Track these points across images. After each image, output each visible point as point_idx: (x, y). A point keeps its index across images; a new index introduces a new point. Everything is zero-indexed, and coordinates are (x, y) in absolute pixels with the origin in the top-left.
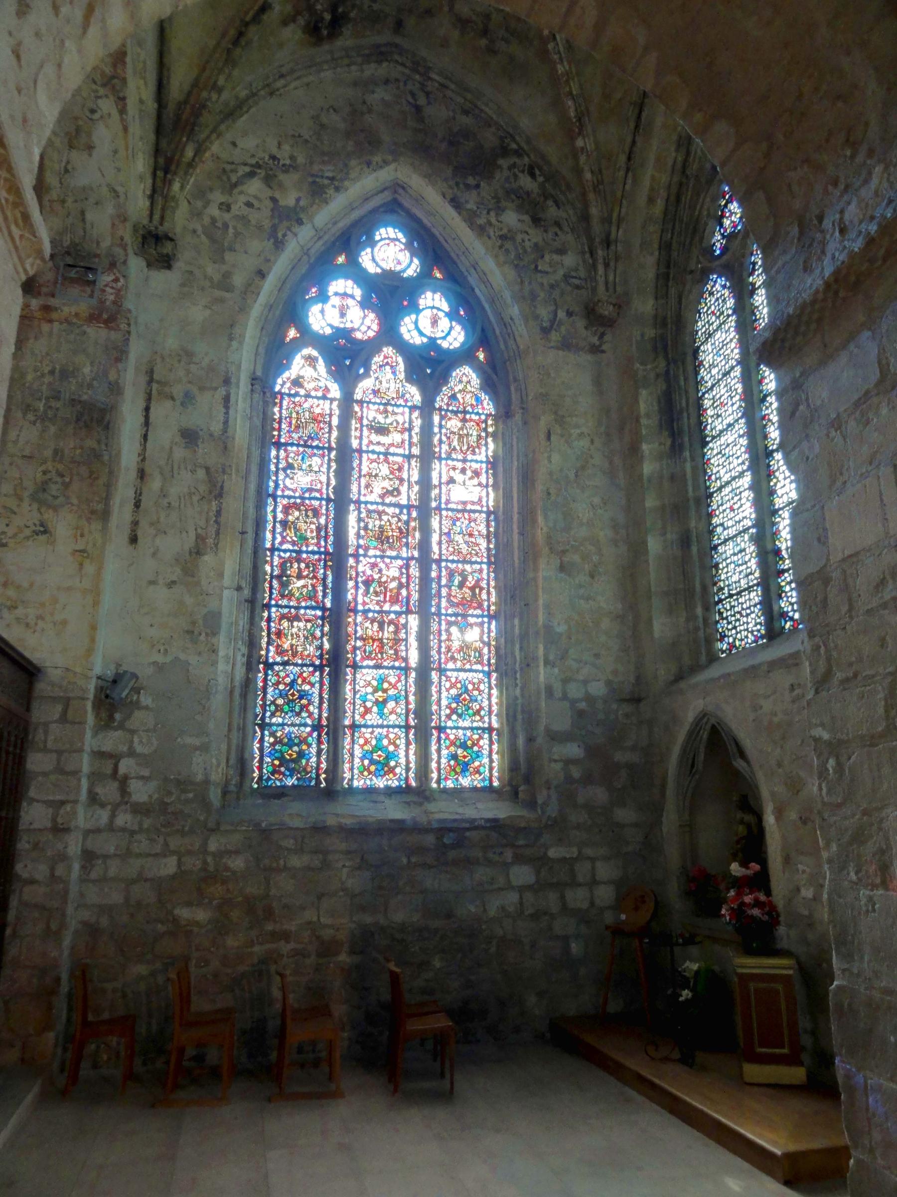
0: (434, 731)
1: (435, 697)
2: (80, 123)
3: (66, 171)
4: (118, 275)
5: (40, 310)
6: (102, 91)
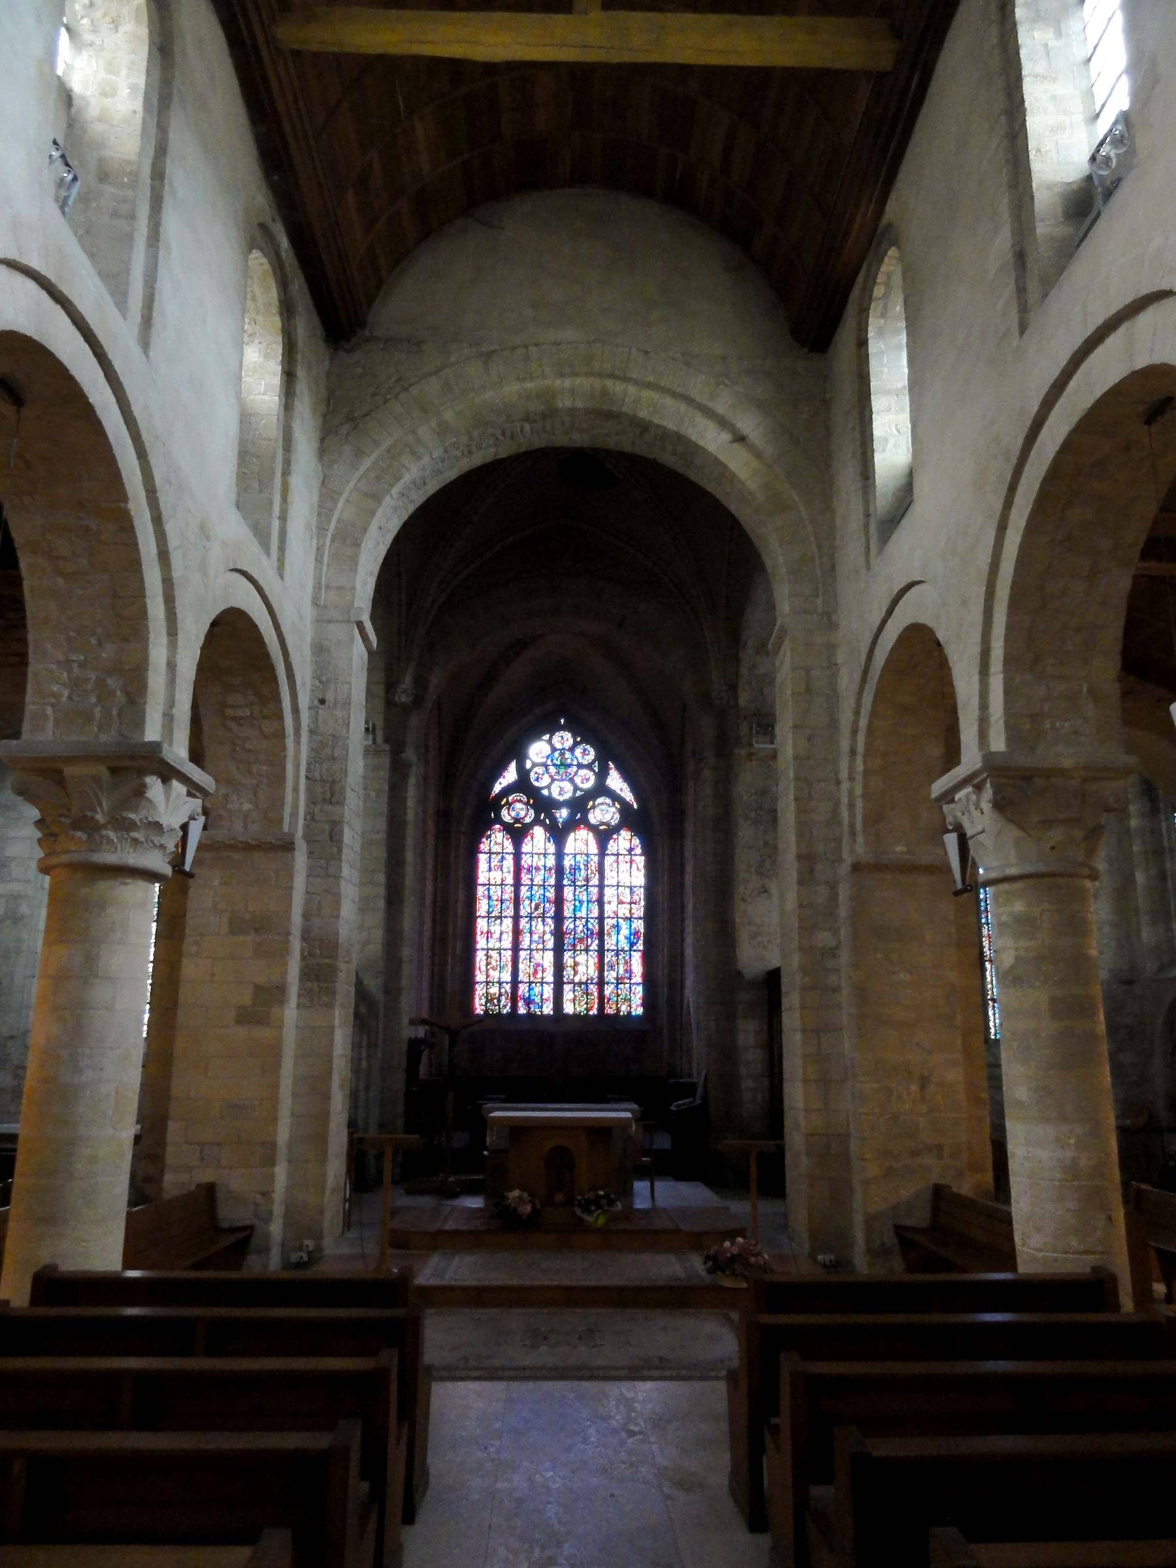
0: (990, 1002)
1: (989, 979)
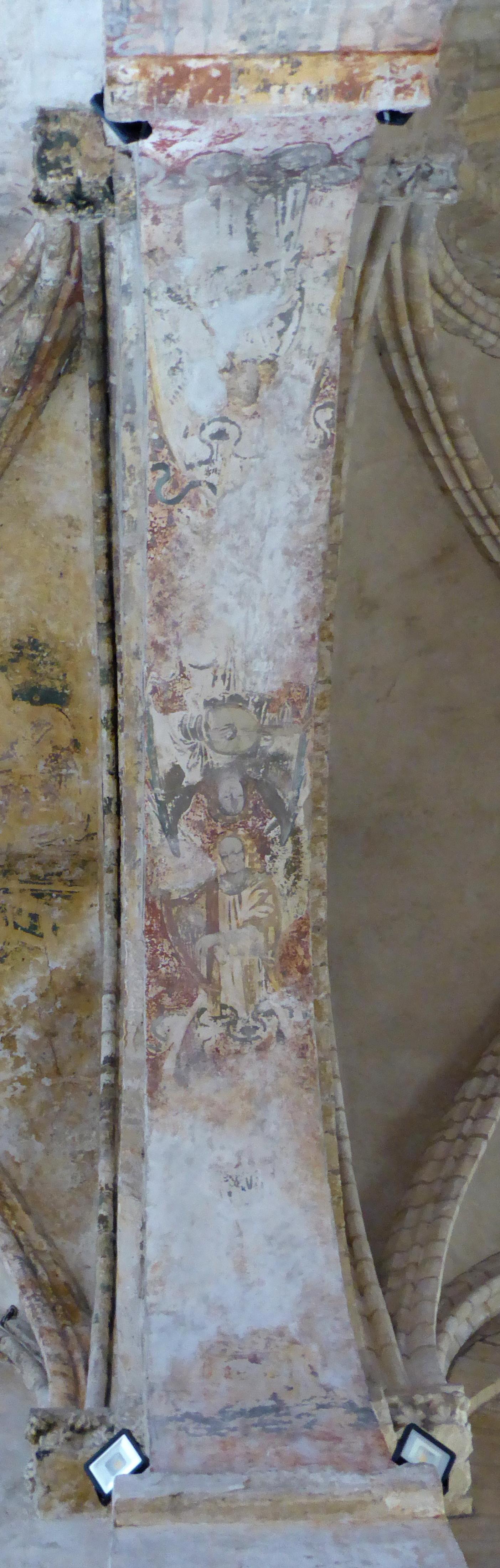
2: (248, 410)
3: (286, 317)
4: (161, 156)
5: (369, 85)
6: (199, 474)
